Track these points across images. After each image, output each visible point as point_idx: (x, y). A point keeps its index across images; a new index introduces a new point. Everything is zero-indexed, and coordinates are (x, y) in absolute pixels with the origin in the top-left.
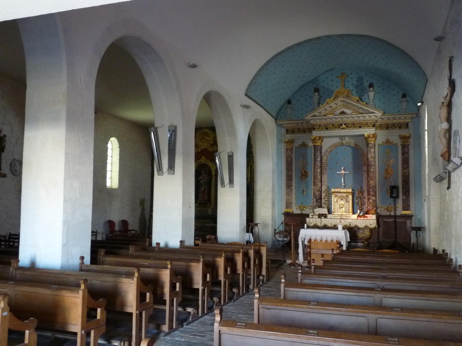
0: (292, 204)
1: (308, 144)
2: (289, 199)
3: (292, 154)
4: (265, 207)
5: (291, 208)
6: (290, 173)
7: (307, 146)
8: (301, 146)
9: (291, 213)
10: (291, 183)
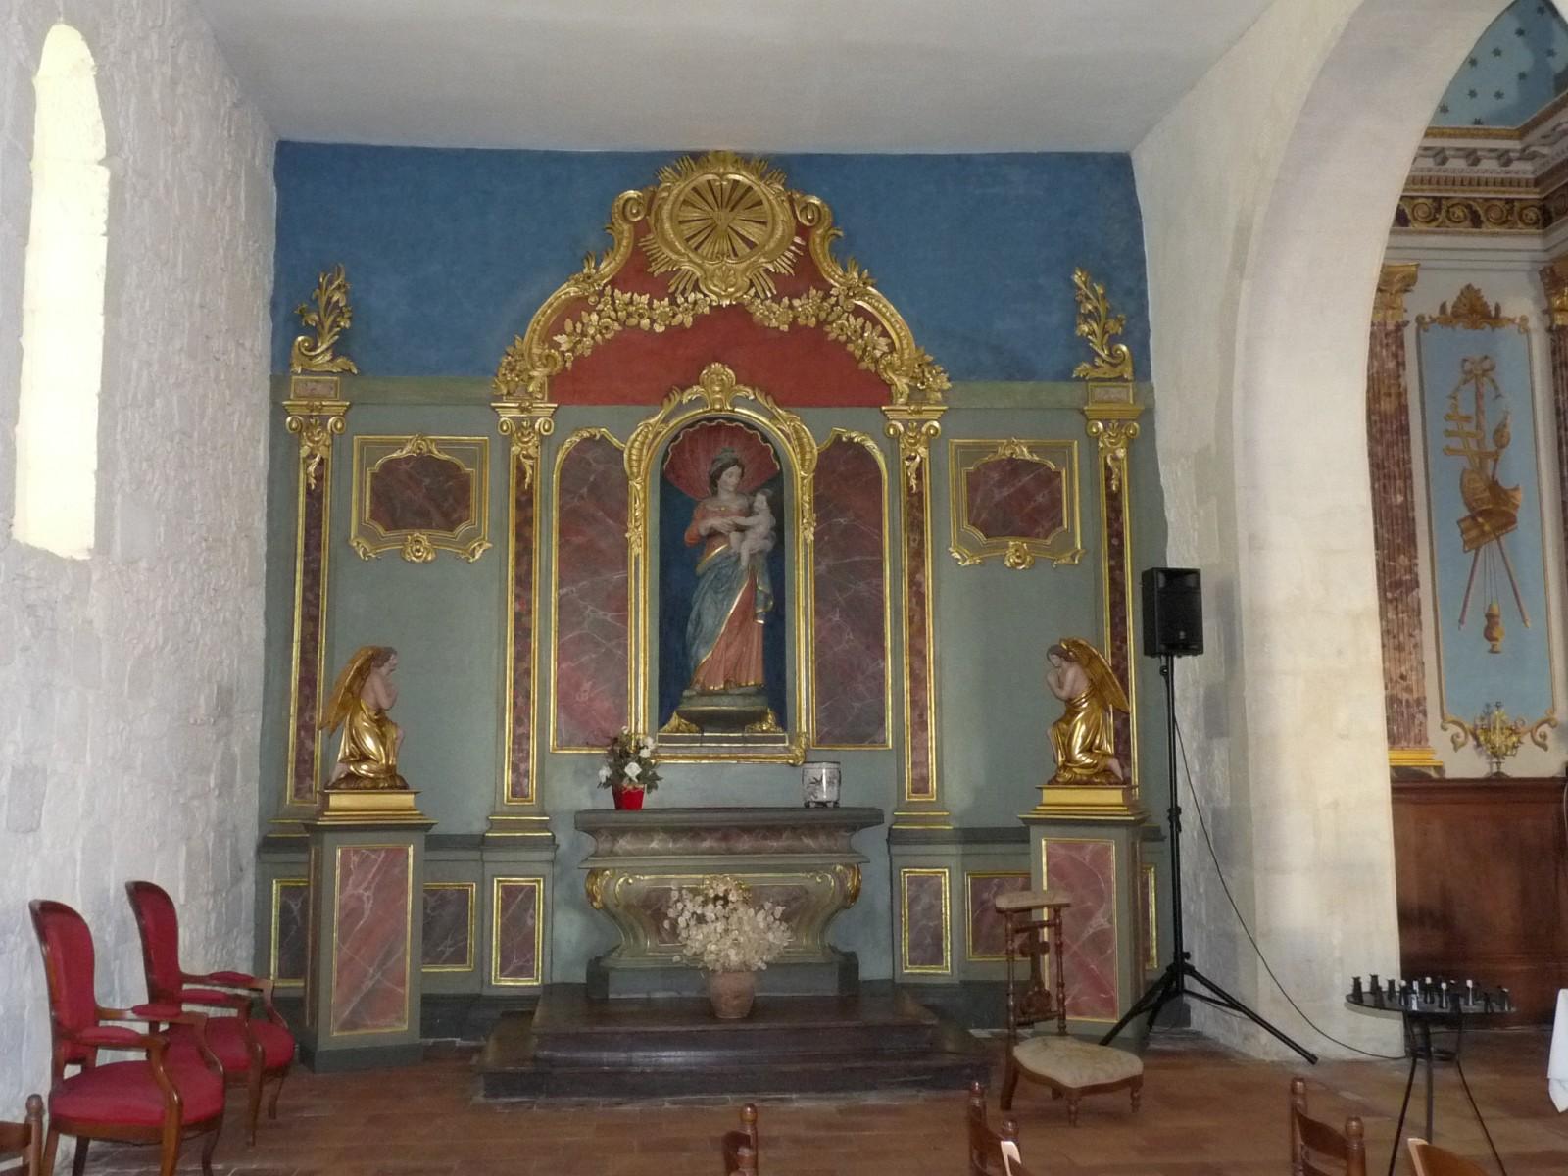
0: (1424, 713)
1: (1498, 308)
2: (1403, 677)
3: (1401, 365)
4: (1342, 737)
5: (1421, 740)
6: (1400, 499)
7: (1497, 316)
8: (1456, 315)
9: (1433, 774)
10: (1411, 569)
